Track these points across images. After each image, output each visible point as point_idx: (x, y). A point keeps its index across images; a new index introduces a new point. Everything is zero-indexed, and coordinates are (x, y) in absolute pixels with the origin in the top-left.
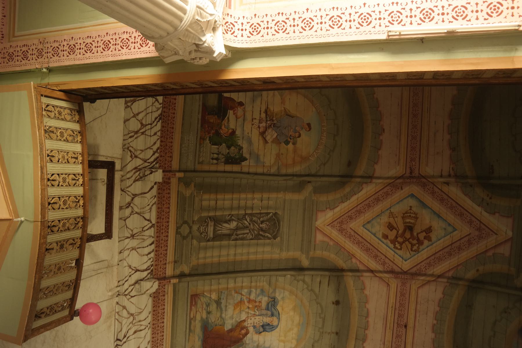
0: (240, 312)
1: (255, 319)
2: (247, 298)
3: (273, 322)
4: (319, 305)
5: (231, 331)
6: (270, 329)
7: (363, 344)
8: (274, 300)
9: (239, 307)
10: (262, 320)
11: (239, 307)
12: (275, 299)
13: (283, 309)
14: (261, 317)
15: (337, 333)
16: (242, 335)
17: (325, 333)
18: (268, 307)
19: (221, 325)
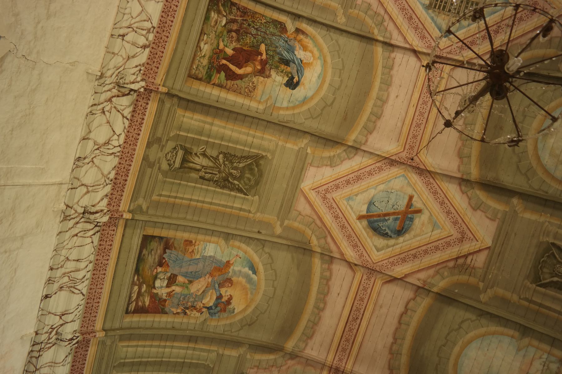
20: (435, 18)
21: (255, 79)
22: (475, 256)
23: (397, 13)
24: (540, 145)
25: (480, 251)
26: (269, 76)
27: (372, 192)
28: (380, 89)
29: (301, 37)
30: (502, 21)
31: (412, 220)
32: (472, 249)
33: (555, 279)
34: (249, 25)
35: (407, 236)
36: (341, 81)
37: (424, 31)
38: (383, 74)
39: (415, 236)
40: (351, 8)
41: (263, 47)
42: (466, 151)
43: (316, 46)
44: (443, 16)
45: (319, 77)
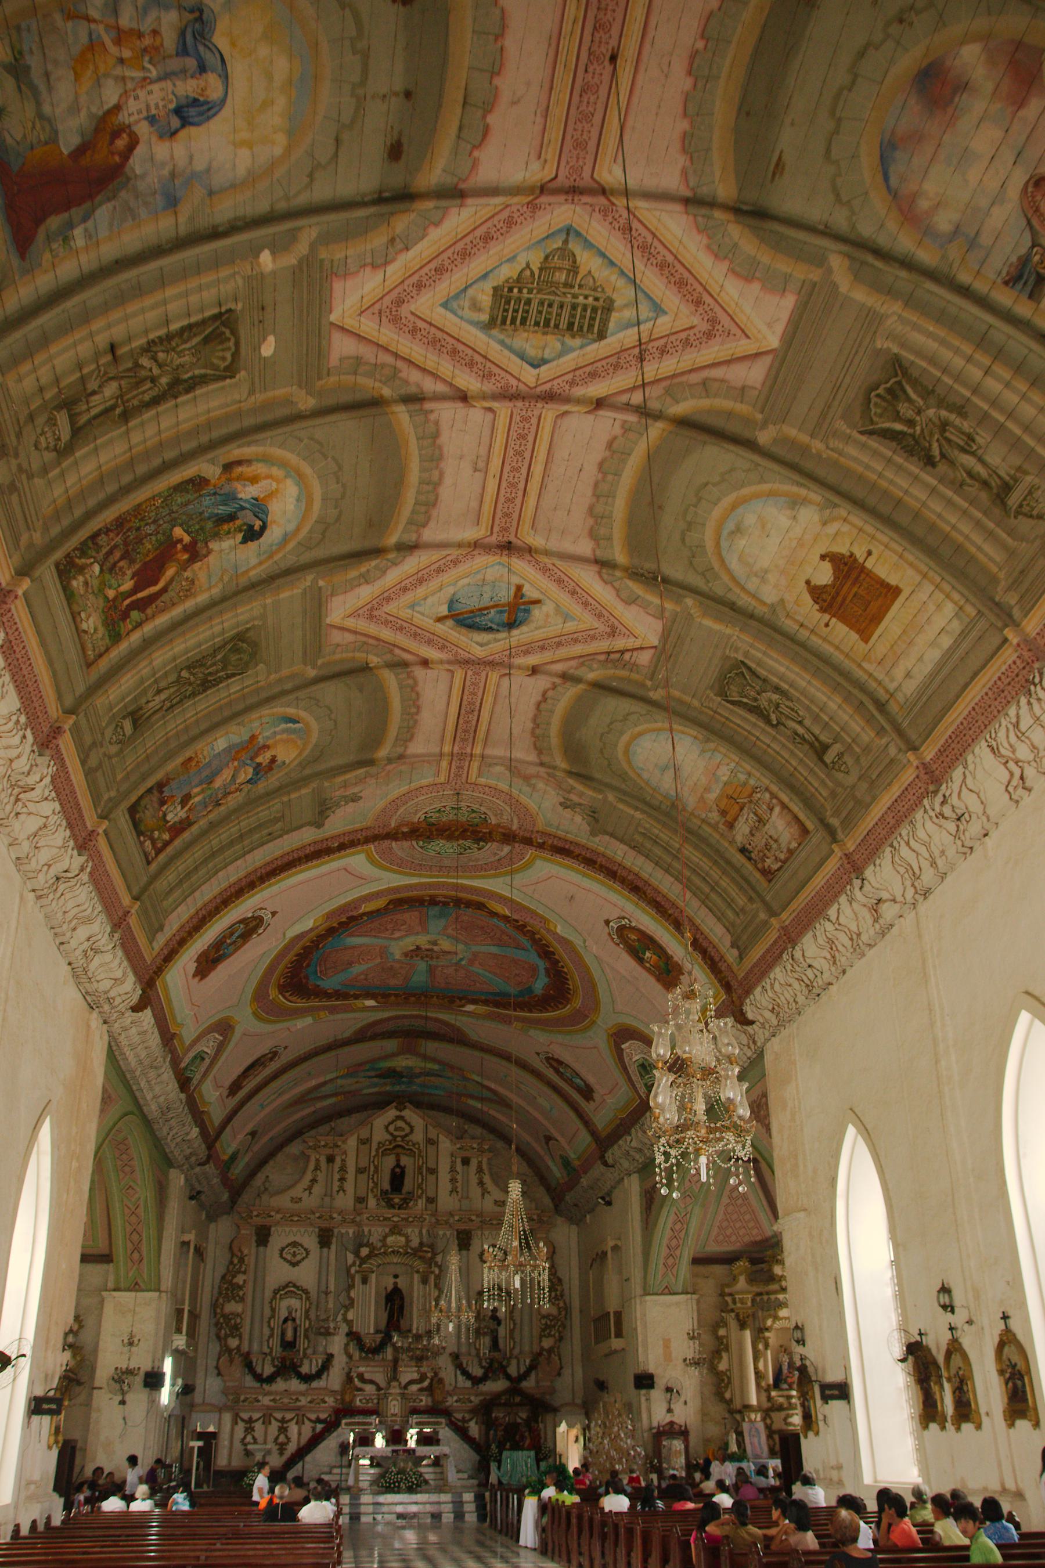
0: (98, 83)
1: (150, 93)
2: (108, 28)
3: (208, 92)
4: (347, 11)
5: (81, 150)
6: (201, 114)
7: (484, 117)
8: (200, 19)
9: (91, 67)
10: (173, 93)
11: (91, 67)
12: (201, 12)
13: (233, 44)
14: (168, 85)
15: (408, 95)
16: (120, 155)
17: (373, 97)
18: (185, 44)
19: (46, 143)
20: (508, 341)
21: (187, 574)
22: (635, 654)
23: (422, 352)
24: (724, 544)
25: (642, 648)
26: (209, 552)
27: (451, 590)
28: (423, 470)
29: (240, 469)
30: (651, 341)
31: (528, 611)
32: (630, 646)
33: (745, 700)
34: (138, 529)
35: (524, 628)
36: (344, 486)
37: (489, 364)
38: (420, 449)
39: (537, 629)
40: (320, 378)
41: (178, 532)
42: (603, 531)
43: (273, 465)
44: (526, 335)
45: (298, 500)
